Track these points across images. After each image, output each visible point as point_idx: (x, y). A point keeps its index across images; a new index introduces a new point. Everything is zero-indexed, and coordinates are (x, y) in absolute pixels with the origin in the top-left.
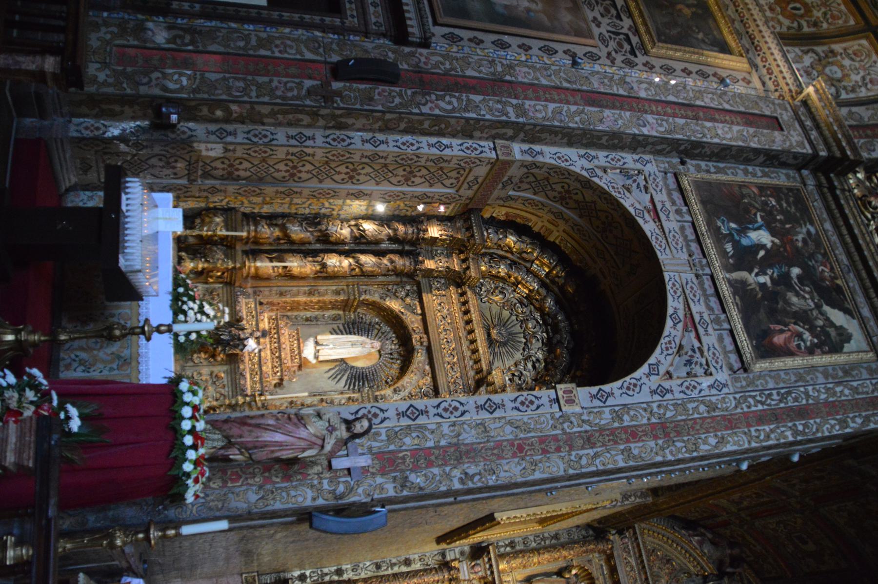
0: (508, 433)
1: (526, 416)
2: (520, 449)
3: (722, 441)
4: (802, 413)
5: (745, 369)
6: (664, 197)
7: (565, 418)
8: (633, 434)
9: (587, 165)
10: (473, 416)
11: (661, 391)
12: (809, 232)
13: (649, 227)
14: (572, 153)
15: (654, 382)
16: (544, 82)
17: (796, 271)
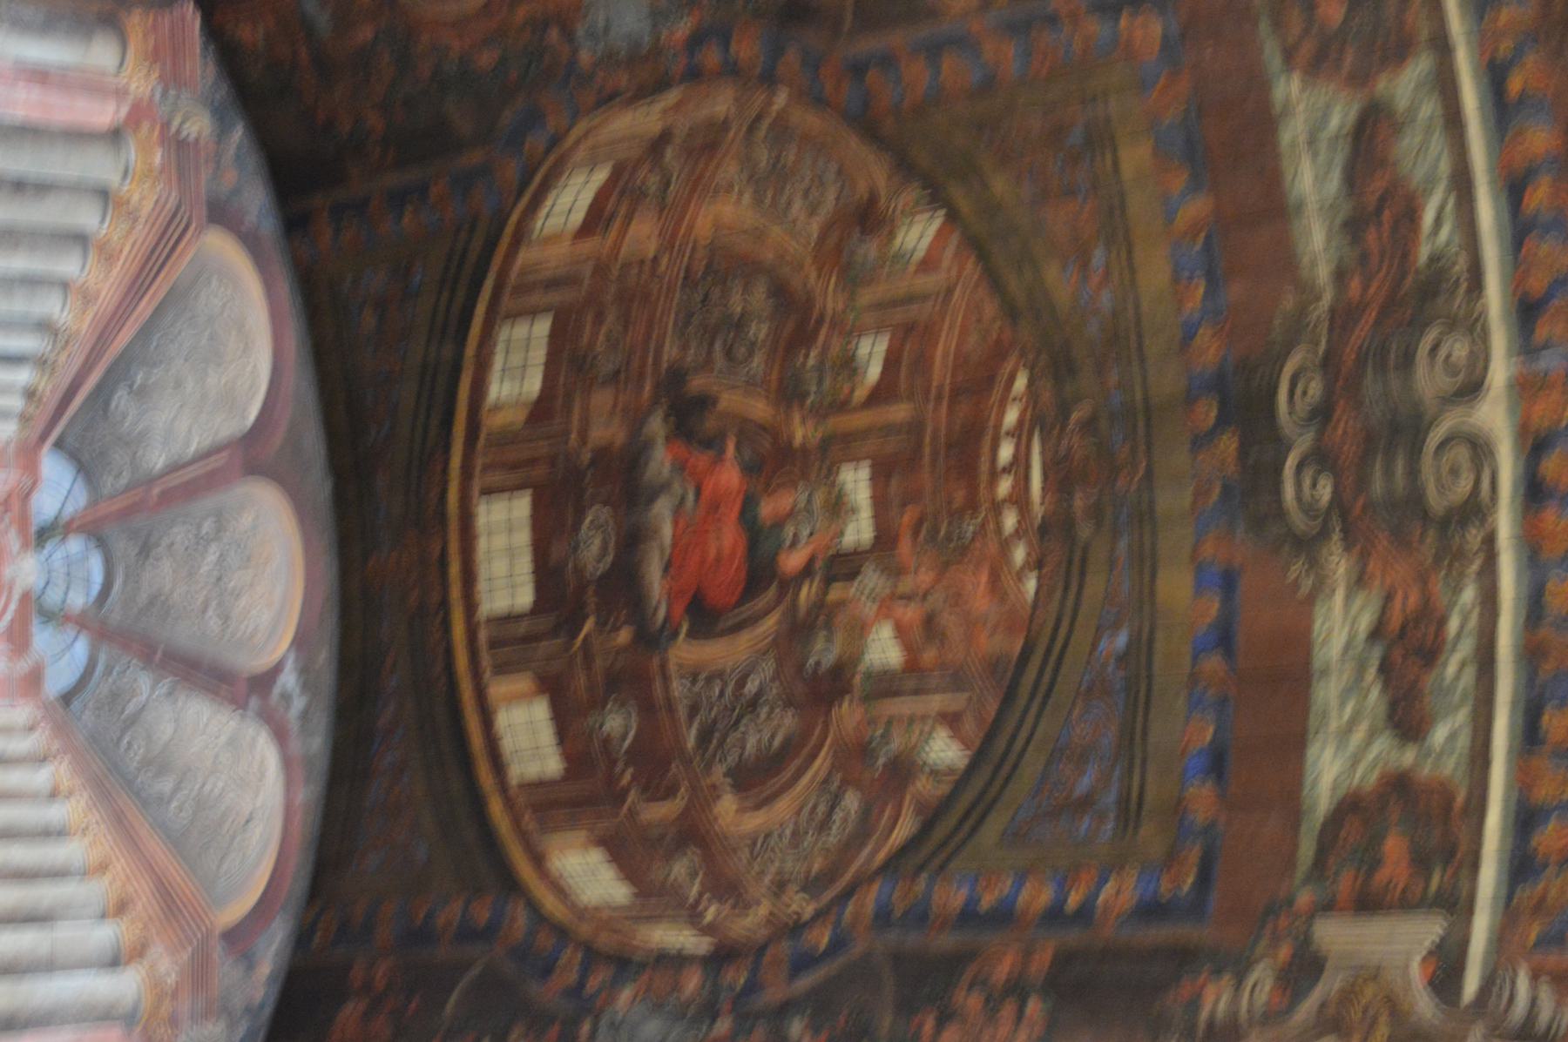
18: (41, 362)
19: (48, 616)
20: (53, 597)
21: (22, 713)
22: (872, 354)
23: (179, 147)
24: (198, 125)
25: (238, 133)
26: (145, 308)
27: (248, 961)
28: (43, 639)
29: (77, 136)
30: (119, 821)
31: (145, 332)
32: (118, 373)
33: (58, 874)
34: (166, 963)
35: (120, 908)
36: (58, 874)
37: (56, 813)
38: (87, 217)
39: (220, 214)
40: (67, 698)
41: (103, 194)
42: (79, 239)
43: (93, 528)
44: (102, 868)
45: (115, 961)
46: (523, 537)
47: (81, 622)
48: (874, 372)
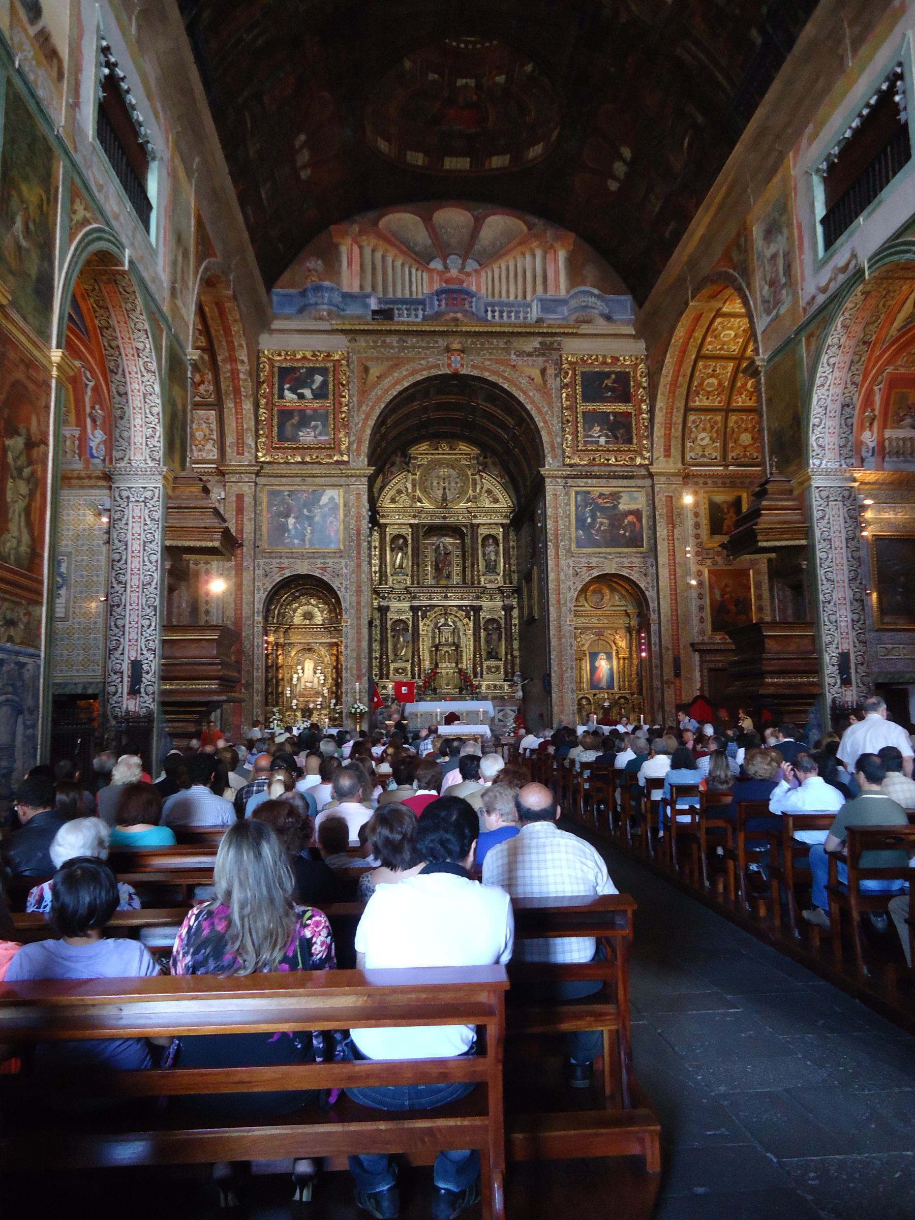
0: (354, 644)
1: (350, 636)
2: (359, 641)
3: (364, 572)
4: (358, 534)
5: (341, 552)
6: (274, 561)
7: (351, 625)
8: (358, 603)
9: (262, 591)
10: (349, 652)
11: (346, 588)
12: (289, 495)
13: (287, 573)
14: (257, 596)
15: (343, 589)
16: (233, 606)
17: (305, 511)
18: (410, 267)
19: (463, 266)
20: (460, 267)
21: (483, 274)
22: (432, 76)
23: (361, 232)
24: (356, 228)
25: (357, 218)
26: (397, 243)
27: (534, 225)
28: (468, 269)
29: (361, 254)
30: (506, 254)
31: (402, 242)
32: (411, 249)
33: (516, 266)
34: (535, 244)
35: (523, 254)
36: (516, 266)
37: (504, 268)
38: (378, 255)
39: (375, 223)
40: (480, 265)
41: (373, 251)
42: (383, 257)
43: (444, 259)
44: (515, 258)
45: (534, 256)
46: (454, 160)
47: (464, 261)
48: (436, 76)
